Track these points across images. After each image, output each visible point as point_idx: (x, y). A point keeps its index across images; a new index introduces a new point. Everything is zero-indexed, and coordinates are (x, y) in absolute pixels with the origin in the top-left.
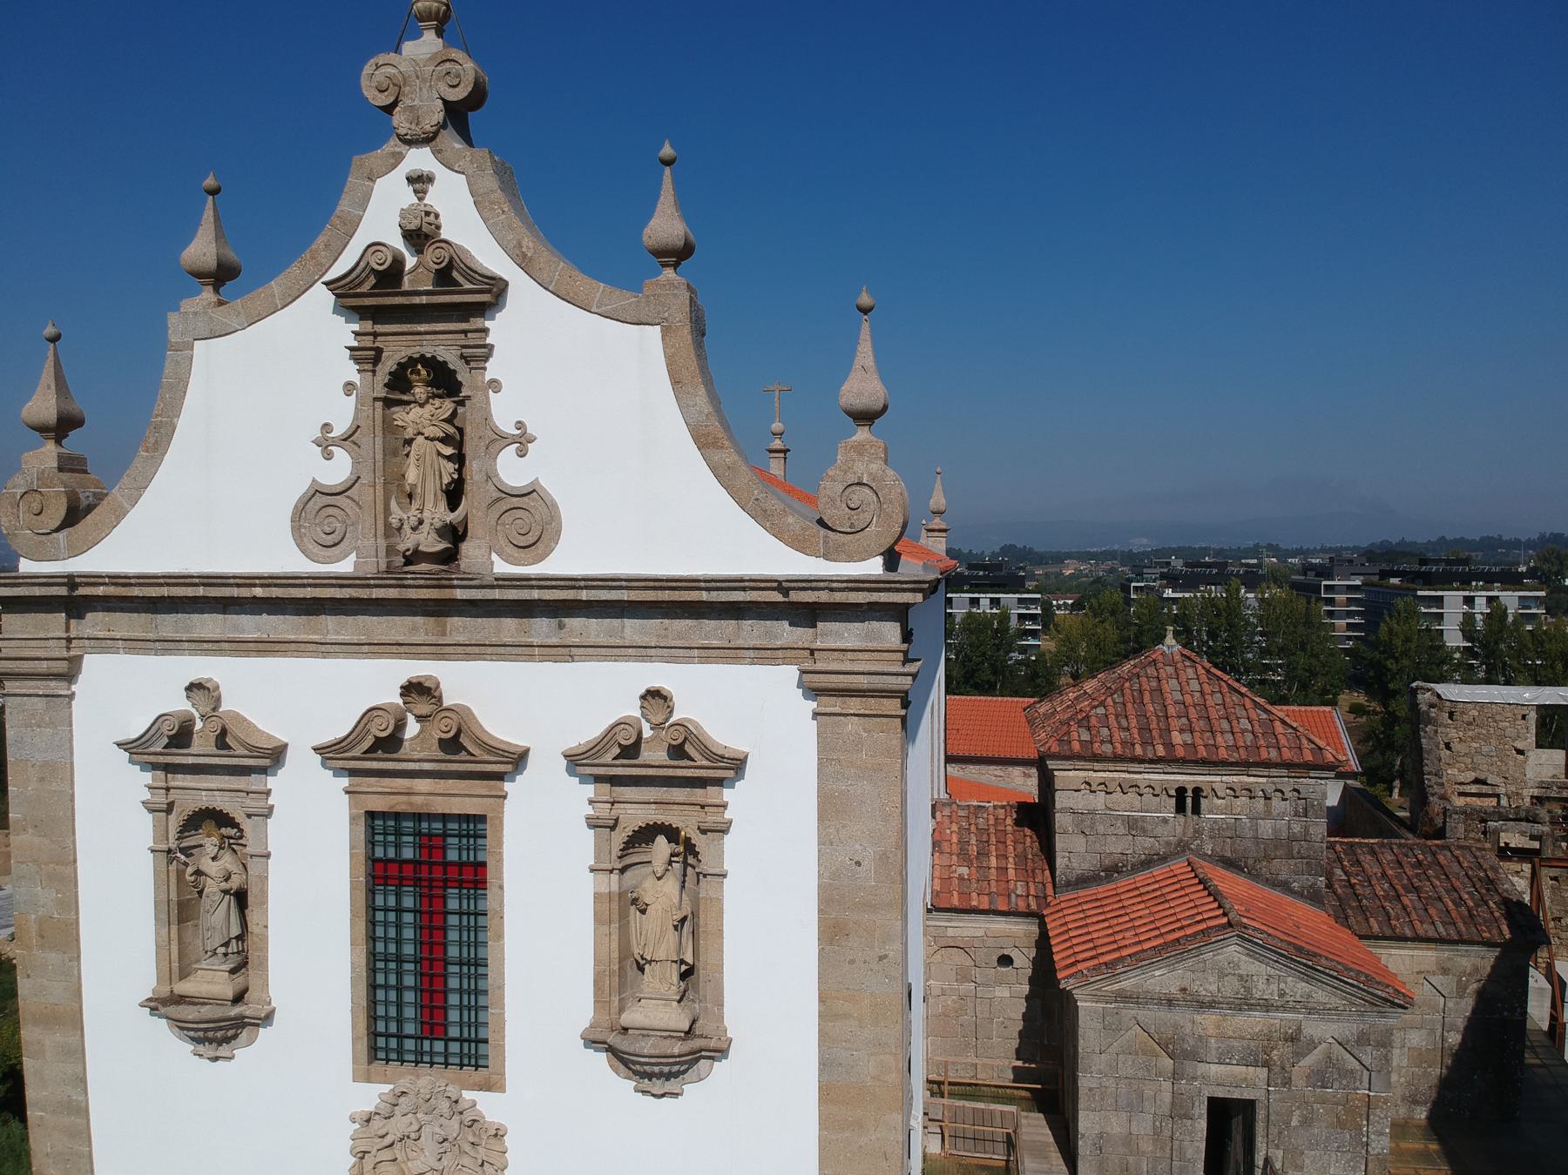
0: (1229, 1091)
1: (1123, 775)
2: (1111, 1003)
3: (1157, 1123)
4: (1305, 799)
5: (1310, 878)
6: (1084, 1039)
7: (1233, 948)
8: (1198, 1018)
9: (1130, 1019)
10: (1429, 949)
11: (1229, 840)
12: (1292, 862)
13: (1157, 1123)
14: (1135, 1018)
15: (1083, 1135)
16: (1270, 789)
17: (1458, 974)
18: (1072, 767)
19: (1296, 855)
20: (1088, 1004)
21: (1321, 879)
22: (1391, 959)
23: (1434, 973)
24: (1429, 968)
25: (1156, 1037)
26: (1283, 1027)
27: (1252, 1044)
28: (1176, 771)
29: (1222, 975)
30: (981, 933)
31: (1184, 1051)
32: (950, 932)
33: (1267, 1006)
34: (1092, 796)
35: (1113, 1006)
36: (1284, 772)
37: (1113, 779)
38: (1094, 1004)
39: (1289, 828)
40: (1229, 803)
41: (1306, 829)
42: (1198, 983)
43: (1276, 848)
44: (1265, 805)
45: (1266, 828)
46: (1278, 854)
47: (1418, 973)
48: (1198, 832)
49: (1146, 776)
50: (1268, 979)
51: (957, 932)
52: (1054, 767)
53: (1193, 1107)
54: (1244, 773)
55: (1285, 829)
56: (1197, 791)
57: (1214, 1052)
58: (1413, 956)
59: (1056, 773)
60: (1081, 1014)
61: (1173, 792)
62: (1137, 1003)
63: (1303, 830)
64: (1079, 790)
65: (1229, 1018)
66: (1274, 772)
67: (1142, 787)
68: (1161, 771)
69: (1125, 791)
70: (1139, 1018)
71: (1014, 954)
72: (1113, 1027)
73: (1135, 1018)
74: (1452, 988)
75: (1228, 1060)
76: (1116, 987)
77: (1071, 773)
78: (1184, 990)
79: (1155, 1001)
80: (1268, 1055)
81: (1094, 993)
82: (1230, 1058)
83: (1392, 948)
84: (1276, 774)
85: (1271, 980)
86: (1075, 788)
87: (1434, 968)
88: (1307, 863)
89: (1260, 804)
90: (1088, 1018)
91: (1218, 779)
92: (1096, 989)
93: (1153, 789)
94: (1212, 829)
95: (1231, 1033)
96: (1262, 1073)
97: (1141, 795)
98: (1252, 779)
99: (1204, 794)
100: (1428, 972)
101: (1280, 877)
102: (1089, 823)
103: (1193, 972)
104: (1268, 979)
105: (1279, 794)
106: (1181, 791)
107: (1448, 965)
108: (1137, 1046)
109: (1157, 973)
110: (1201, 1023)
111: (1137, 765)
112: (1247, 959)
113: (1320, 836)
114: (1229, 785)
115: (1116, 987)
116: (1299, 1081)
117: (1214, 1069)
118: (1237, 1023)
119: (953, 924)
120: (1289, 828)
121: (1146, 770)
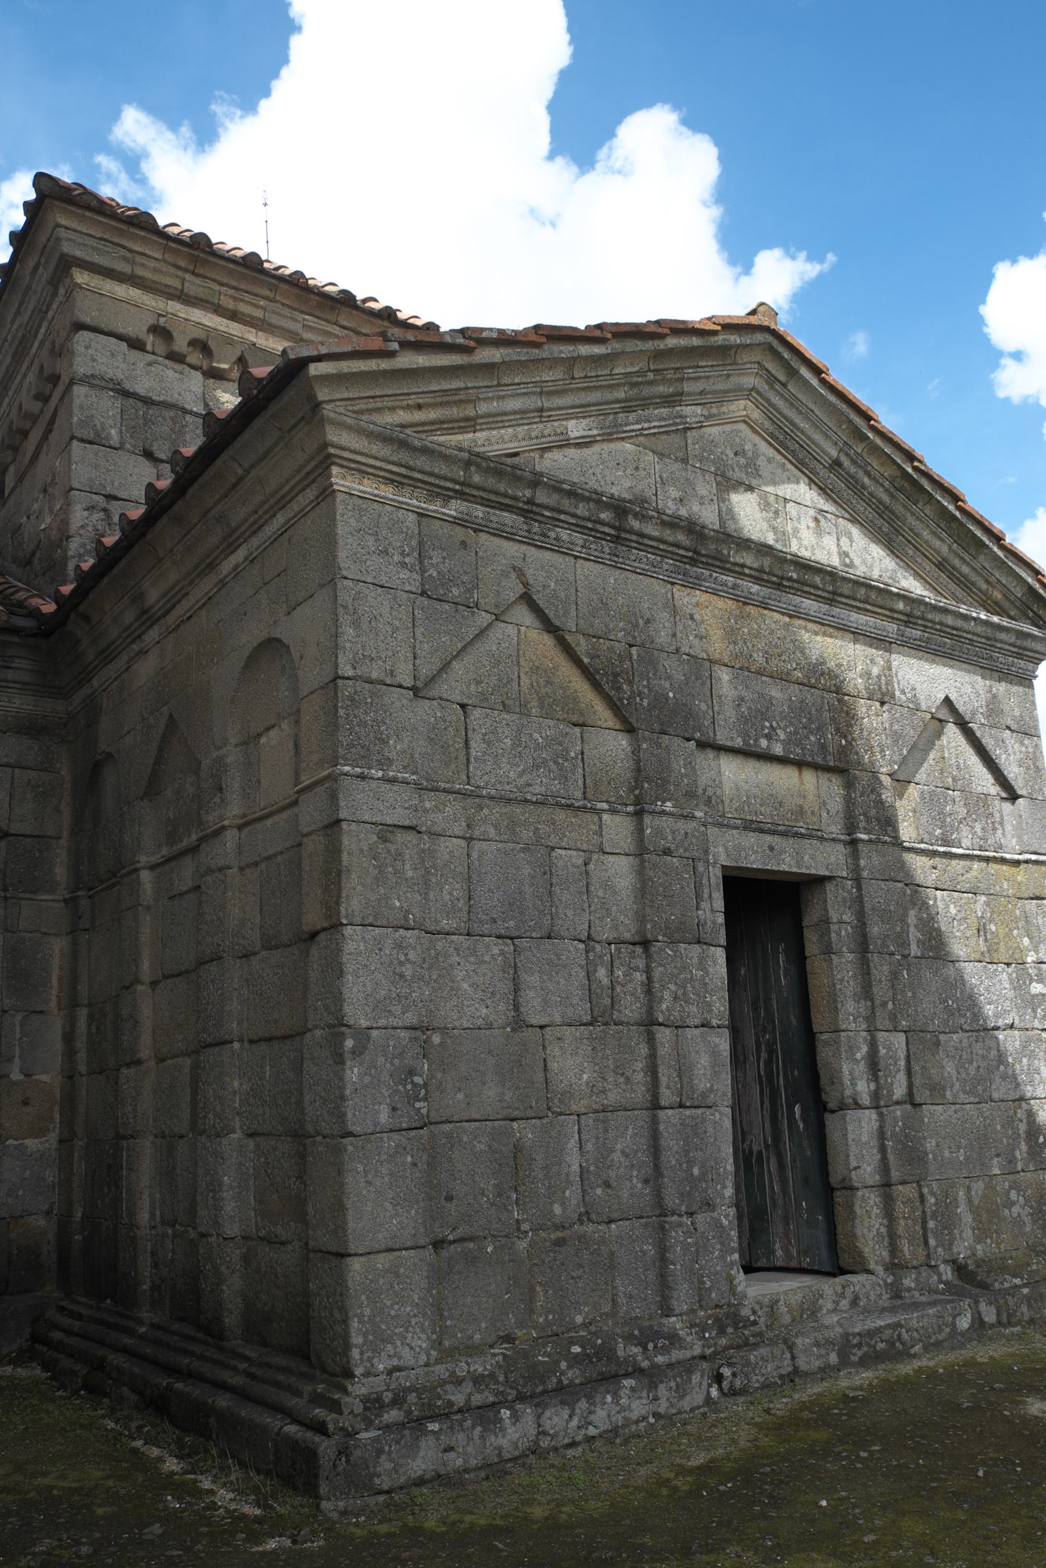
0: (771, 849)
1: (252, 336)
2: (446, 500)
3: (602, 973)
6: (356, 624)
7: (740, 407)
8: (685, 598)
9: (505, 574)
13: (602, 973)
15: (363, 1036)
20: (368, 487)
25: (582, 646)
27: (810, 697)
31: (659, 700)
34: (170, 373)
35: (453, 509)
37: (228, 340)
38: (387, 491)
42: (674, 493)
53: (698, 897)
57: (730, 713)
62: (529, 511)
65: (752, 610)
70: (529, 572)
72: (455, 591)
73: (520, 574)
77: (121, 290)
79: (582, 510)
80: (845, 737)
82: (768, 737)
86: (130, 331)
90: (371, 541)
102: (165, 429)
103: (661, 455)
104: (816, 520)
108: (525, 681)
109: (576, 429)
110: (692, 618)
112: (771, 452)
118: (772, 632)
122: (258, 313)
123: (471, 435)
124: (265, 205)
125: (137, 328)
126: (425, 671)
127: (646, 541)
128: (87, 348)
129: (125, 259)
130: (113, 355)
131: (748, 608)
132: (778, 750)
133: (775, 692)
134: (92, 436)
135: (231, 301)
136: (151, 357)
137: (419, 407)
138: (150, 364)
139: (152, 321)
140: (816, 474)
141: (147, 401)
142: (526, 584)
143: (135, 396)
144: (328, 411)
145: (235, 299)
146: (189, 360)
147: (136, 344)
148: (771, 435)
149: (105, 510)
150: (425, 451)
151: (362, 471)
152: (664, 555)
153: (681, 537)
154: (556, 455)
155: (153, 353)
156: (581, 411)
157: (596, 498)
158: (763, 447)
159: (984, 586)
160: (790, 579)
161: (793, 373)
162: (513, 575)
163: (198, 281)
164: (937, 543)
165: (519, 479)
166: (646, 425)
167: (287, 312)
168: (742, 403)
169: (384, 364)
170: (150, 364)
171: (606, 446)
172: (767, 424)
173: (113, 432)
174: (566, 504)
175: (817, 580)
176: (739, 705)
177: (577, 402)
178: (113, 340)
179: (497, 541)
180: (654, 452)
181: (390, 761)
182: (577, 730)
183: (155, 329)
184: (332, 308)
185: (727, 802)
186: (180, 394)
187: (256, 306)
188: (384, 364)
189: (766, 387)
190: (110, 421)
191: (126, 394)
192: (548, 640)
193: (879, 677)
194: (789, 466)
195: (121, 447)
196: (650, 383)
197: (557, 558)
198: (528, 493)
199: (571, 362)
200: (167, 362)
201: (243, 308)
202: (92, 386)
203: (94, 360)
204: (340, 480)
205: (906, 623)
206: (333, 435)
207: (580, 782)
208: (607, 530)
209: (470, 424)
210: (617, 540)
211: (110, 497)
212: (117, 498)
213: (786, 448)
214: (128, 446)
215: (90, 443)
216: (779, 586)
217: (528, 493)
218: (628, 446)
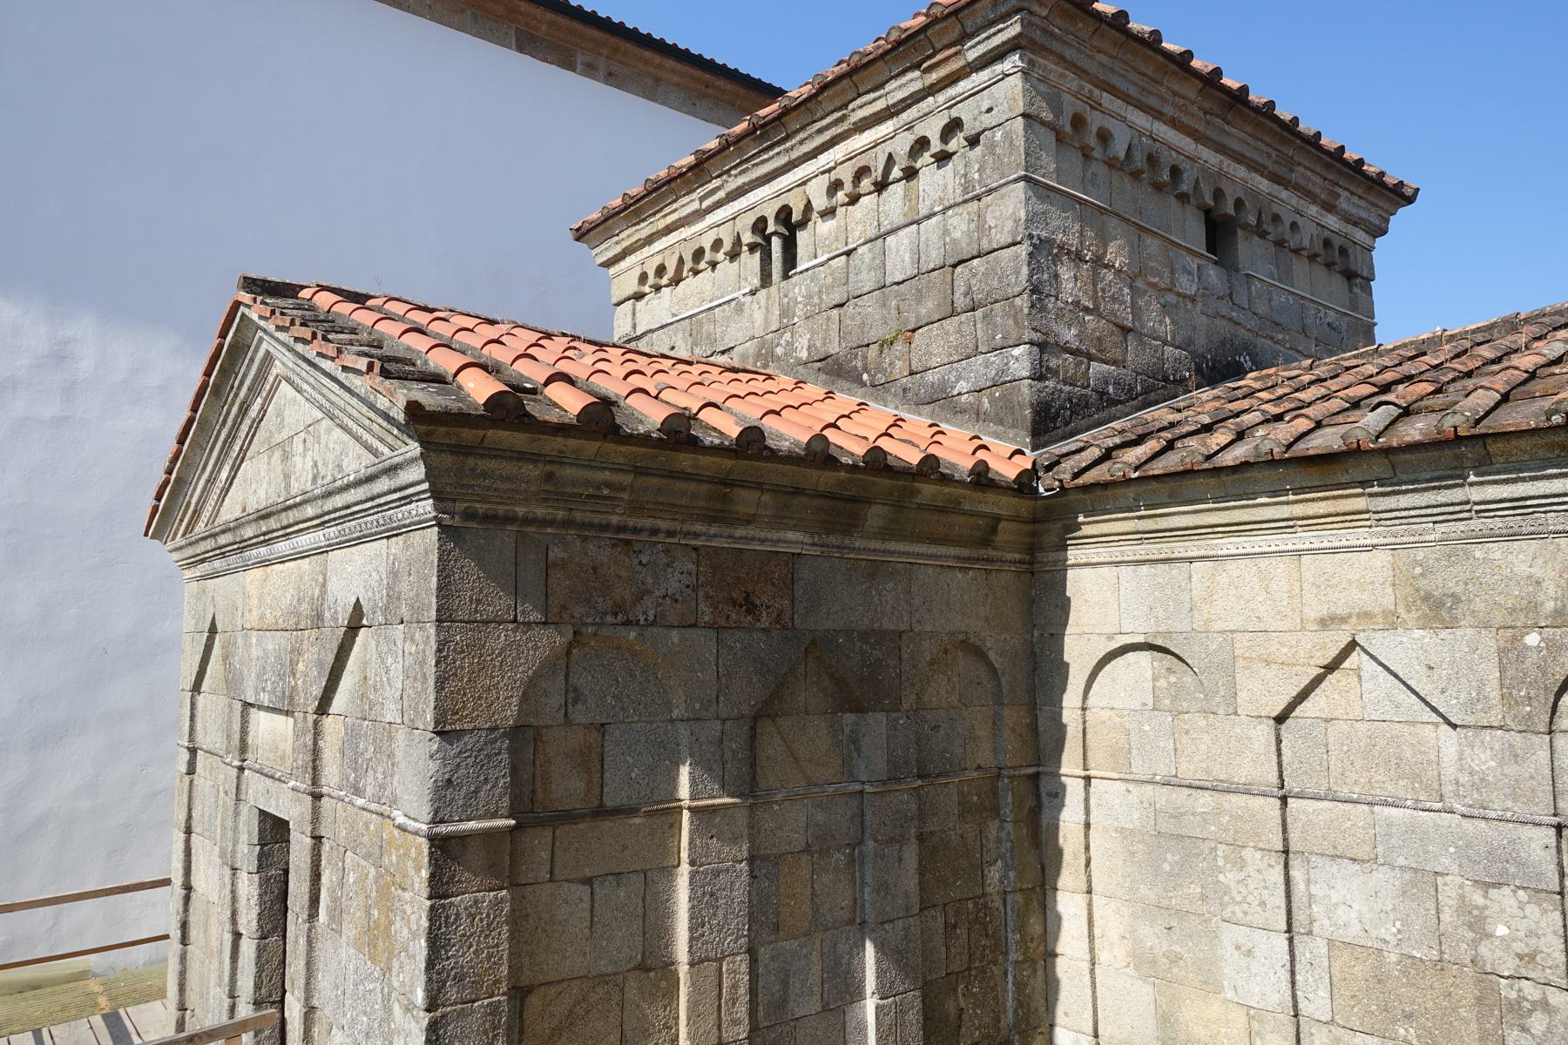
5: (992, 357)
11: (835, 311)
12: (949, 324)
17: (1498, 618)
18: (618, 249)
19: (961, 302)
21: (1016, 351)
22: (1223, 579)
23: (1391, 622)
24: (1364, 600)
36: (913, 82)
39: (946, 232)
40: (843, 223)
43: (920, 297)
45: (900, 254)
46: (923, 311)
47: (1325, 623)
48: (786, 312)
54: (845, 126)
55: (935, 238)
56: (784, 214)
58: (1299, 553)
61: (747, 238)
63: (973, 226)
66: (897, 90)
68: (721, 194)
74: (1482, 683)
84: (900, 95)
87: (1388, 599)
88: (985, 317)
94: (809, 297)
100: (1366, 615)
101: (931, 377)
105: (927, 157)
107: (1447, 580)
111: (686, 199)
113: (1010, 224)
120: (946, 232)
121: (706, 204)
129: (617, 243)
147: (639, 296)
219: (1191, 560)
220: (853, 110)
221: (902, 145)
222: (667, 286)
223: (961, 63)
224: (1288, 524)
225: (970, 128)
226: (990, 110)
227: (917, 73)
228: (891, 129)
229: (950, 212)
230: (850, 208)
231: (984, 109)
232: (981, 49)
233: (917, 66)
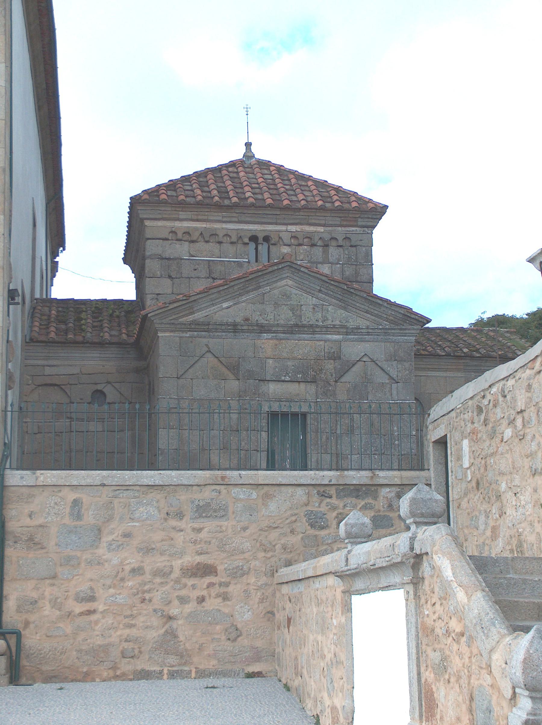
1: (204, 225)
2: (186, 332)
4: (355, 246)
7: (283, 282)
10: (458, 370)
14: (207, 345)
16: (327, 237)
18: (160, 216)
20: (167, 334)
26: (327, 348)
28: (249, 219)
29: (276, 305)
30: (76, 371)
32: (48, 371)
33: (312, 329)
37: (196, 229)
38: (172, 334)
41: (357, 273)
44: (324, 252)
49: (224, 226)
50: (313, 308)
51: (54, 371)
52: (145, 216)
56: (266, 239)
58: (446, 377)
59: (147, 223)
60: (161, 342)
61: (246, 240)
62: (208, 331)
63: (354, 272)
64: (167, 239)
67: (221, 235)
68: (236, 220)
69: (207, 239)
71: (108, 390)
73: (207, 345)
75: (283, 378)
76: (190, 318)
77: (160, 223)
78: (247, 320)
79: (223, 327)
81: (172, 321)
82: (285, 376)
83: (429, 369)
84: (330, 223)
85: (316, 308)
86: (163, 236)
89: (318, 252)
91: (283, 228)
92: (173, 319)
93: (230, 237)
95: (285, 355)
96: (312, 388)
97: (220, 243)
98: (312, 229)
99: (273, 242)
103: (254, 304)
104: (313, 308)
105: (334, 243)
106: (254, 239)
108: (209, 371)
109: (225, 305)
110: (261, 347)
114: (293, 234)
115: (190, 318)
116: (342, 396)
117: (273, 388)
119: (51, 362)
121: (225, 219)
122: (206, 218)
123: (194, 315)
124: (247, 114)
125: (165, 234)
126: (181, 373)
127: (244, 331)
128: (149, 246)
129: (160, 214)
130: (157, 246)
131: (282, 341)
132: (288, 378)
133: (290, 363)
134: (152, 276)
135: (196, 216)
136: (172, 241)
137: (177, 314)
138: (171, 244)
139: (170, 230)
140: (314, 295)
141: (169, 259)
142: (209, 348)
143: (166, 259)
144: (155, 321)
145: (196, 215)
146: (184, 239)
148: (296, 287)
149: (157, 299)
150: (179, 324)
151: (165, 331)
152: (250, 333)
153: (255, 328)
154: (221, 313)
155: (172, 240)
156: (226, 300)
157: (227, 324)
158: (294, 291)
159: (385, 316)
160: (296, 331)
161: (299, 270)
162: (205, 346)
163: (184, 213)
164: (363, 306)
165: (204, 324)
166: (248, 298)
167: (216, 214)
168: (285, 281)
169: (166, 309)
170: (171, 244)
171: (236, 306)
172: (296, 285)
173: (158, 272)
174: (218, 327)
175: (306, 329)
176: (275, 369)
177: (224, 299)
178: (158, 240)
179: (201, 339)
180: (252, 303)
181: (171, 394)
182: (223, 381)
183: (172, 232)
184: (232, 209)
185: (270, 394)
186: (181, 252)
187: (205, 215)
188: (166, 309)
189: (292, 275)
190: (157, 269)
191: (162, 259)
192: (216, 360)
193: (334, 352)
194: (304, 294)
195: (161, 276)
196: (248, 287)
197: (218, 340)
198: (207, 327)
199: (219, 292)
200: (176, 242)
201: (200, 217)
202: (151, 259)
203: (152, 249)
204: (160, 334)
205: (347, 335)
206: (157, 326)
207: (223, 394)
208: (231, 330)
209: (193, 313)
210: (235, 332)
211: (158, 294)
212: (160, 294)
213: (303, 290)
214: (163, 276)
215: (152, 278)
216: (292, 333)
217: (207, 327)
218: (243, 304)
219: (421, 376)
220: (311, 219)
221: (327, 237)
222: (185, 241)
223: (356, 224)
224: (446, 370)
225: (353, 243)
226: (361, 240)
227: (339, 219)
228: (323, 230)
229: (346, 265)
230: (297, 247)
231: (359, 239)
232: (364, 224)
233: (340, 217)
